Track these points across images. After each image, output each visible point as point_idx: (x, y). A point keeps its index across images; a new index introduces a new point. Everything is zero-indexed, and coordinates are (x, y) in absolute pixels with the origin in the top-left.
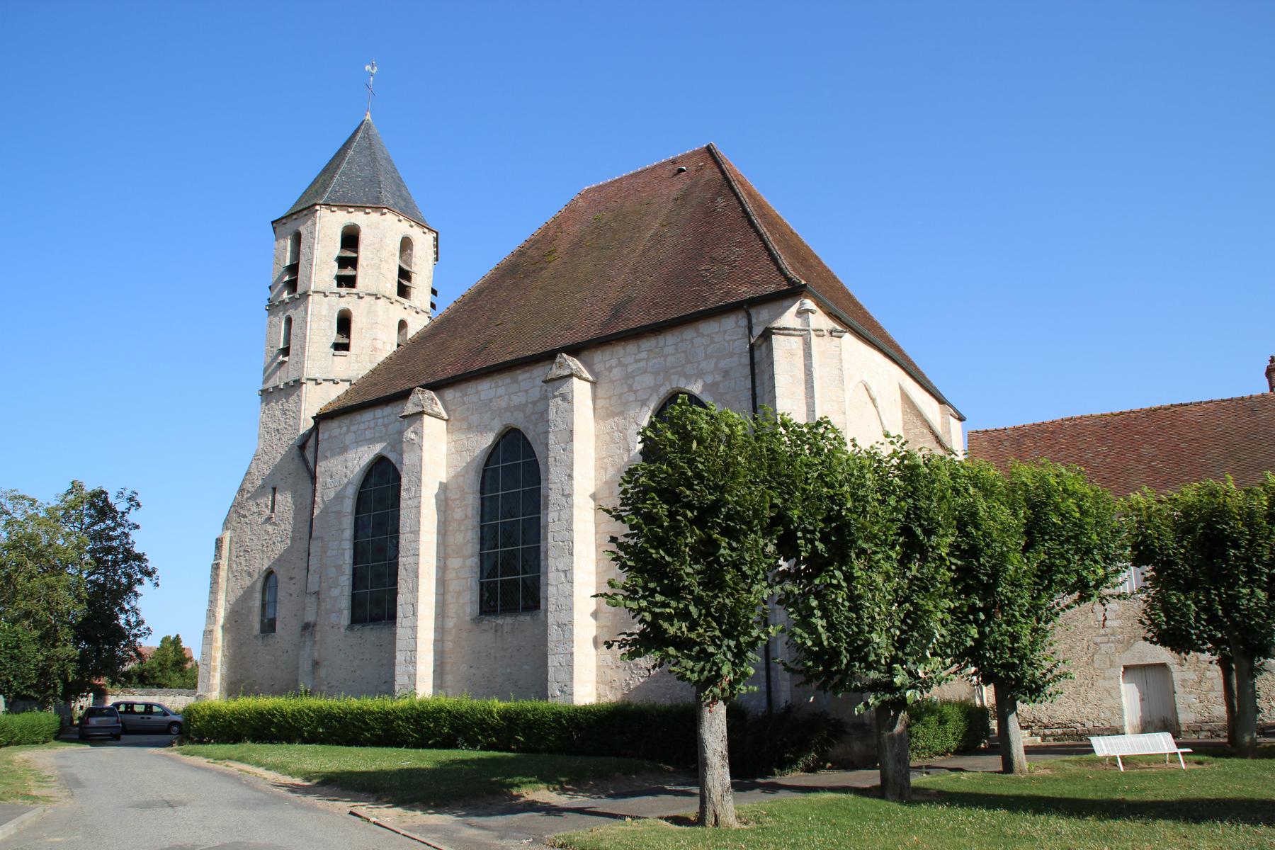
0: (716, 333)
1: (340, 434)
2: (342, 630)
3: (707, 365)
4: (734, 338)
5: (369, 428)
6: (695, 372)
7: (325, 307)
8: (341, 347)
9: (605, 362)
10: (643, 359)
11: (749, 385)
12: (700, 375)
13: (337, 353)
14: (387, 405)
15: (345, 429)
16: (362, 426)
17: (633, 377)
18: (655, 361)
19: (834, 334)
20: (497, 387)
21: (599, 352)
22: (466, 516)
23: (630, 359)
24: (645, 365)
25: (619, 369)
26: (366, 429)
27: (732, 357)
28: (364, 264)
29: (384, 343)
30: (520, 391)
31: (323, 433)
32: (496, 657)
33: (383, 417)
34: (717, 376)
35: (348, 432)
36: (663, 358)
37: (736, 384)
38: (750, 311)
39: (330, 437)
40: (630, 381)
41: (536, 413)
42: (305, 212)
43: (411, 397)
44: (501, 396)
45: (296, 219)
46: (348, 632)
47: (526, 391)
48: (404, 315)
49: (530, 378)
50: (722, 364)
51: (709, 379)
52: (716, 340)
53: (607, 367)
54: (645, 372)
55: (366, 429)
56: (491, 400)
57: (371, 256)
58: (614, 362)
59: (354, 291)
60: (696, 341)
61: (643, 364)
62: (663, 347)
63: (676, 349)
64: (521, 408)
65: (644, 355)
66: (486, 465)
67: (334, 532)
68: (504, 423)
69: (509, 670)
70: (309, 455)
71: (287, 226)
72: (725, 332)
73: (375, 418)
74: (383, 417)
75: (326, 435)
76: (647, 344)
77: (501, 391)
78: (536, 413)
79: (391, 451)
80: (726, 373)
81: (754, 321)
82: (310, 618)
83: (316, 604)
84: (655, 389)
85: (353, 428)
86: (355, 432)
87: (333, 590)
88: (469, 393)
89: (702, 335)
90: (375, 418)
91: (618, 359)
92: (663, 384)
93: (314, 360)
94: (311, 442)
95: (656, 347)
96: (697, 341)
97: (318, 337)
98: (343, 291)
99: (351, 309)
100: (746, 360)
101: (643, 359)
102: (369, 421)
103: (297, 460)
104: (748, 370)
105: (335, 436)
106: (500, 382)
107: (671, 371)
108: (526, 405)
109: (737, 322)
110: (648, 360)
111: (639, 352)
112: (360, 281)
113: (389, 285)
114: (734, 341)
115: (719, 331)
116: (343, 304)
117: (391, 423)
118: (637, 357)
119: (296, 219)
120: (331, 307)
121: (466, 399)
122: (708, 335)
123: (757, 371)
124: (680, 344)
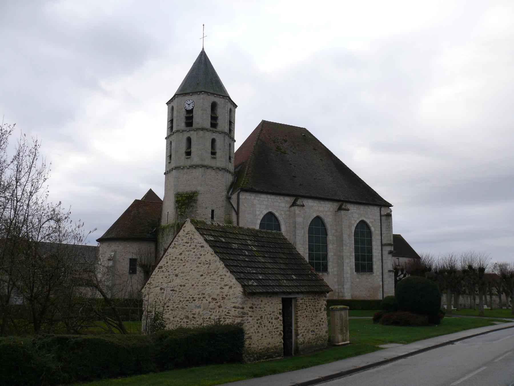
11: (380, 224)
12: (369, 218)
15: (253, 197)
16: (261, 199)
17: (353, 213)
35: (255, 199)
42: (221, 97)
44: (315, 206)
45: (215, 97)
47: (323, 207)
49: (324, 203)
55: (263, 201)
56: (312, 206)
61: (355, 211)
65: (355, 208)
74: (271, 199)
75: (244, 197)
77: (316, 204)
78: (327, 215)
79: (276, 212)
80: (375, 220)
84: (358, 218)
85: (256, 198)
86: (258, 200)
89: (370, 209)
90: (267, 198)
92: (360, 218)
96: (369, 210)
102: (265, 198)
103: (225, 202)
105: (248, 199)
106: (315, 202)
107: (362, 215)
108: (324, 211)
117: (275, 202)
119: (215, 97)
122: (371, 209)
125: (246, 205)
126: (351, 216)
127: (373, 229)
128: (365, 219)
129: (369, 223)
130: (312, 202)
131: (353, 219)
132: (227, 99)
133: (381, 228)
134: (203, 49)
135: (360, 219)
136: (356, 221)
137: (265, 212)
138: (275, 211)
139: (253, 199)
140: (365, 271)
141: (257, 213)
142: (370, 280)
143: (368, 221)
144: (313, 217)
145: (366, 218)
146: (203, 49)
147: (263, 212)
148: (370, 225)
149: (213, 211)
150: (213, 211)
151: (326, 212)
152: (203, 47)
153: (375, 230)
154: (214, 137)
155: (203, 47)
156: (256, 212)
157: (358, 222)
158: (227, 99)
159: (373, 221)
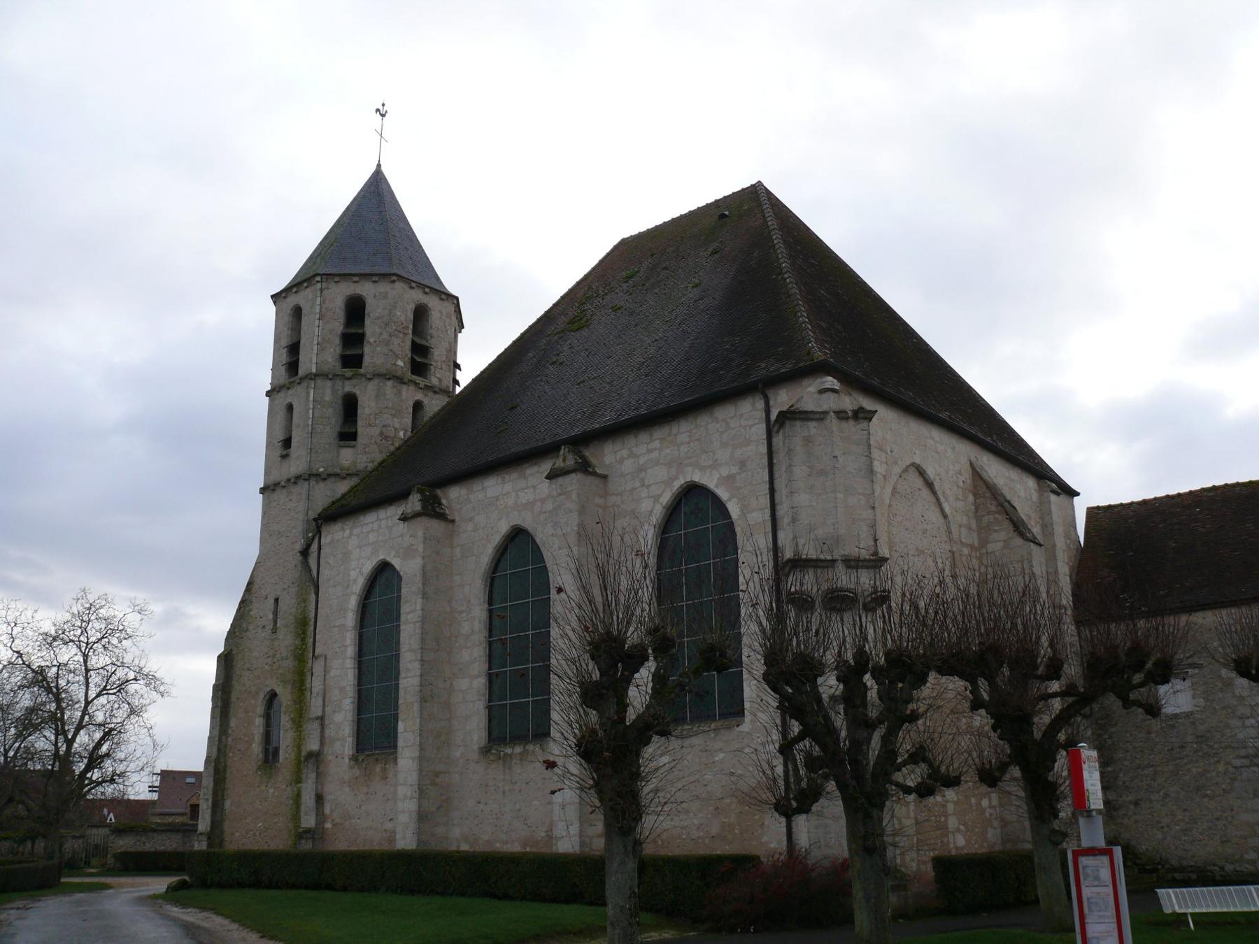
0: (732, 418)
1: (343, 537)
2: (347, 760)
3: (724, 455)
4: (751, 422)
5: (372, 531)
6: (711, 462)
7: (328, 392)
8: (348, 436)
9: (615, 452)
10: (655, 449)
13: (342, 443)
14: (391, 505)
15: (347, 532)
18: (668, 451)
19: (861, 415)
20: (503, 483)
21: (610, 442)
22: (473, 631)
23: (642, 449)
24: (658, 455)
25: (631, 460)
26: (369, 532)
27: (748, 445)
28: (372, 340)
29: (396, 429)
30: (527, 487)
31: (326, 536)
32: (504, 792)
33: (387, 518)
34: (733, 468)
36: (676, 448)
37: (753, 476)
38: (767, 392)
39: (333, 540)
40: (642, 475)
41: (545, 512)
42: (305, 284)
43: (411, 497)
44: (508, 493)
45: (296, 292)
46: (352, 763)
47: (534, 487)
48: (419, 396)
49: (538, 472)
50: (738, 453)
51: (725, 472)
52: (732, 426)
53: (618, 458)
54: (657, 463)
55: (369, 532)
56: (497, 498)
57: (378, 330)
58: (625, 453)
59: (362, 371)
60: (710, 427)
61: (655, 455)
62: (676, 435)
63: (690, 436)
64: (529, 505)
65: (656, 444)
66: (494, 571)
67: (337, 649)
68: (512, 524)
69: (518, 807)
70: (312, 562)
71: (288, 300)
72: (742, 415)
73: (378, 519)
76: (660, 433)
77: (508, 487)
78: (545, 512)
79: (395, 557)
80: (743, 464)
81: (772, 403)
82: (313, 745)
83: (319, 730)
84: (668, 482)
85: (356, 531)
86: (358, 535)
87: (337, 714)
88: (475, 490)
90: (378, 519)
91: (630, 449)
92: (676, 478)
93: (317, 452)
94: (314, 546)
95: (669, 435)
97: (321, 427)
98: (348, 372)
99: (358, 392)
100: (764, 449)
101: (655, 449)
102: (372, 523)
104: (765, 461)
106: (507, 477)
109: (753, 405)
110: (660, 449)
111: (652, 441)
112: (367, 360)
113: (400, 363)
114: (751, 426)
115: (735, 416)
116: (349, 387)
118: (649, 447)
120: (334, 392)
121: (472, 496)
122: (724, 420)
123: (775, 461)
124: (694, 431)
125: (331, 561)
126: (638, 484)
127: (734, 509)
128: (697, 477)
129: (717, 486)
130: (497, 484)
131: (644, 492)
132: (318, 282)
133: (772, 491)
134: (379, 165)
135: (677, 484)
136: (656, 499)
137: (368, 567)
138: (393, 553)
139: (348, 537)
140: (710, 718)
141: (353, 574)
142: (722, 755)
143: (710, 481)
144: (497, 539)
145: (702, 469)
146: (379, 165)
147: (363, 570)
148: (723, 494)
149: (277, 600)
150: (277, 600)
151: (543, 501)
152: (379, 161)
153: (744, 514)
154: (289, 400)
155: (379, 161)
156: (349, 575)
157: (667, 498)
158: (318, 282)
159: (734, 470)
